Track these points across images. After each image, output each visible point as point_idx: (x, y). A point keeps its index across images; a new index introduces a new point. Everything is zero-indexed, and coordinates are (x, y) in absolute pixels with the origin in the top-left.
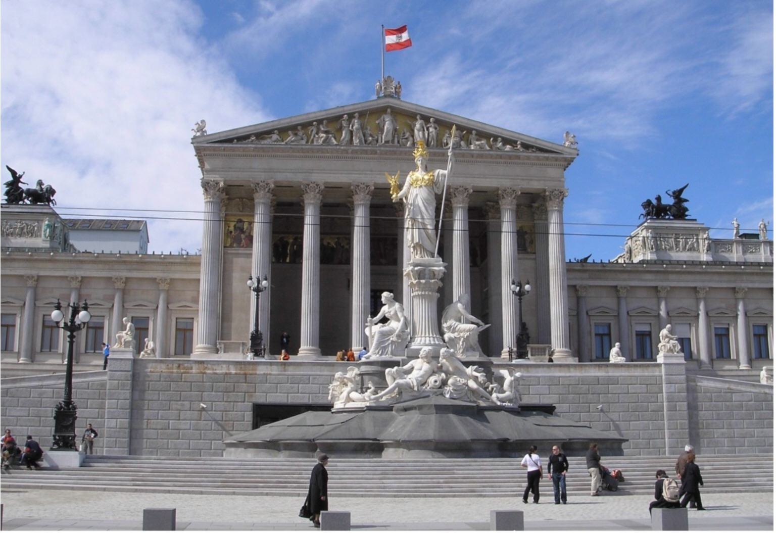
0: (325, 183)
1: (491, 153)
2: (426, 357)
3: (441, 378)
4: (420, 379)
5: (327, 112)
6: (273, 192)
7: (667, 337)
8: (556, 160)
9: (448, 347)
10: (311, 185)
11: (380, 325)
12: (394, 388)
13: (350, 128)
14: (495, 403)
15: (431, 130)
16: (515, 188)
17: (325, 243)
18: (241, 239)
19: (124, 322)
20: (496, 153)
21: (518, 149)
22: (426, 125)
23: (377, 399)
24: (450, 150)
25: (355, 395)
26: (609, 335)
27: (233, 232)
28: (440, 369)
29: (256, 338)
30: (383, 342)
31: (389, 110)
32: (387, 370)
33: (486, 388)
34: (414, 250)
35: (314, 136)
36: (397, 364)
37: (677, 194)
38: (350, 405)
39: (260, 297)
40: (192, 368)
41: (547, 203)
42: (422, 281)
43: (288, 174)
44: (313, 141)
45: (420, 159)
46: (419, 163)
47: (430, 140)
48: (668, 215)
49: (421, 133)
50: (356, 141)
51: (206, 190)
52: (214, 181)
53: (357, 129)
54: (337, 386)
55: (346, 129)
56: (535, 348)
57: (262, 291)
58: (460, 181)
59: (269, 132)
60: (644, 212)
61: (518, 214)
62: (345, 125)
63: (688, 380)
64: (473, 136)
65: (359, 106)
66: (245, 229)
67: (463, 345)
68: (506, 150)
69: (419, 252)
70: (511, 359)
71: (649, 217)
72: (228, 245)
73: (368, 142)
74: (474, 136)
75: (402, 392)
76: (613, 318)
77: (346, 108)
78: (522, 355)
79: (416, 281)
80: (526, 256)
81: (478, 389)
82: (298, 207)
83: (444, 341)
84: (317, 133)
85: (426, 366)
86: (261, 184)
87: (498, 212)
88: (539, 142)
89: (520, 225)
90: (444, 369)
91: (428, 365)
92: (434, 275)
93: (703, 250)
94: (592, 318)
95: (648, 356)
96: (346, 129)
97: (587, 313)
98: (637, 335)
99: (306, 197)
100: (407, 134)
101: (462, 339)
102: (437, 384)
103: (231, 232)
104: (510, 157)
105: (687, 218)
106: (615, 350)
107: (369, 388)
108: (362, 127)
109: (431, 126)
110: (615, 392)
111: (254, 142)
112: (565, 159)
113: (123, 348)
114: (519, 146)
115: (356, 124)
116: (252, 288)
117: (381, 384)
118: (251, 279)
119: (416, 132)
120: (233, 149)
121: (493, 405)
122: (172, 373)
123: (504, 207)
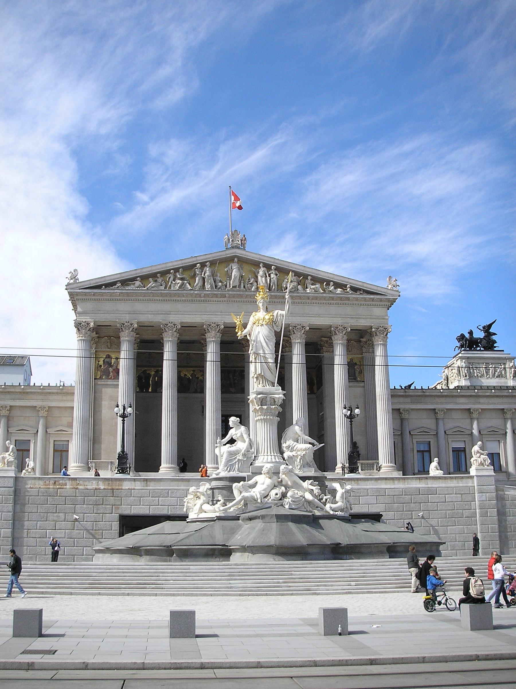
0: (181, 323)
1: (325, 295)
2: (268, 473)
3: (281, 491)
4: (263, 492)
5: (183, 262)
6: (137, 331)
7: (478, 452)
8: (381, 300)
9: (287, 465)
10: (169, 325)
11: (228, 445)
12: (241, 500)
13: (203, 275)
14: (329, 513)
15: (272, 276)
16: (346, 325)
17: (182, 375)
18: (109, 372)
19: (7, 445)
20: (328, 295)
21: (348, 292)
22: (268, 272)
23: (225, 510)
24: (288, 293)
25: (206, 507)
26: (429, 451)
27: (103, 366)
28: (280, 483)
29: (122, 457)
30: (231, 460)
32: (235, 485)
33: (320, 500)
34: (257, 381)
35: (172, 283)
36: (243, 479)
37: (487, 329)
38: (203, 515)
39: (125, 422)
40: (66, 485)
41: (373, 338)
42: (264, 407)
45: (262, 301)
46: (261, 305)
48: (479, 346)
49: (263, 278)
50: (208, 286)
51: (78, 329)
52: (85, 322)
53: (208, 276)
54: (191, 499)
55: (199, 276)
56: (365, 464)
57: (127, 417)
58: (296, 320)
59: (133, 279)
60: (458, 345)
61: (349, 348)
62: (198, 273)
63: (497, 490)
64: (309, 281)
66: (112, 364)
67: (300, 462)
68: (337, 293)
69: (261, 382)
70: (344, 474)
71: (463, 349)
72: (98, 377)
73: (218, 287)
75: (247, 504)
76: (432, 436)
77: (198, 258)
78: (353, 469)
79: (259, 407)
80: (356, 384)
81: (313, 500)
82: (159, 344)
83: (284, 459)
84: (174, 280)
85: (268, 481)
86: (126, 324)
87: (331, 346)
88: (365, 285)
90: (283, 483)
91: (270, 479)
92: (275, 402)
93: (510, 377)
95: (464, 469)
96: (199, 276)
98: (453, 451)
99: (165, 335)
100: (252, 280)
101: (300, 457)
102: (278, 496)
103: (101, 366)
104: (341, 299)
105: (495, 349)
106: (434, 464)
107: (219, 501)
108: (213, 275)
109: (272, 273)
110: (434, 501)
111: (119, 288)
112: (389, 300)
113: (6, 468)
114: (348, 289)
115: (208, 271)
116: (119, 415)
117: (230, 497)
118: (118, 406)
119: (259, 277)
120: (102, 294)
121: (327, 514)
122: (49, 488)
123: (336, 341)
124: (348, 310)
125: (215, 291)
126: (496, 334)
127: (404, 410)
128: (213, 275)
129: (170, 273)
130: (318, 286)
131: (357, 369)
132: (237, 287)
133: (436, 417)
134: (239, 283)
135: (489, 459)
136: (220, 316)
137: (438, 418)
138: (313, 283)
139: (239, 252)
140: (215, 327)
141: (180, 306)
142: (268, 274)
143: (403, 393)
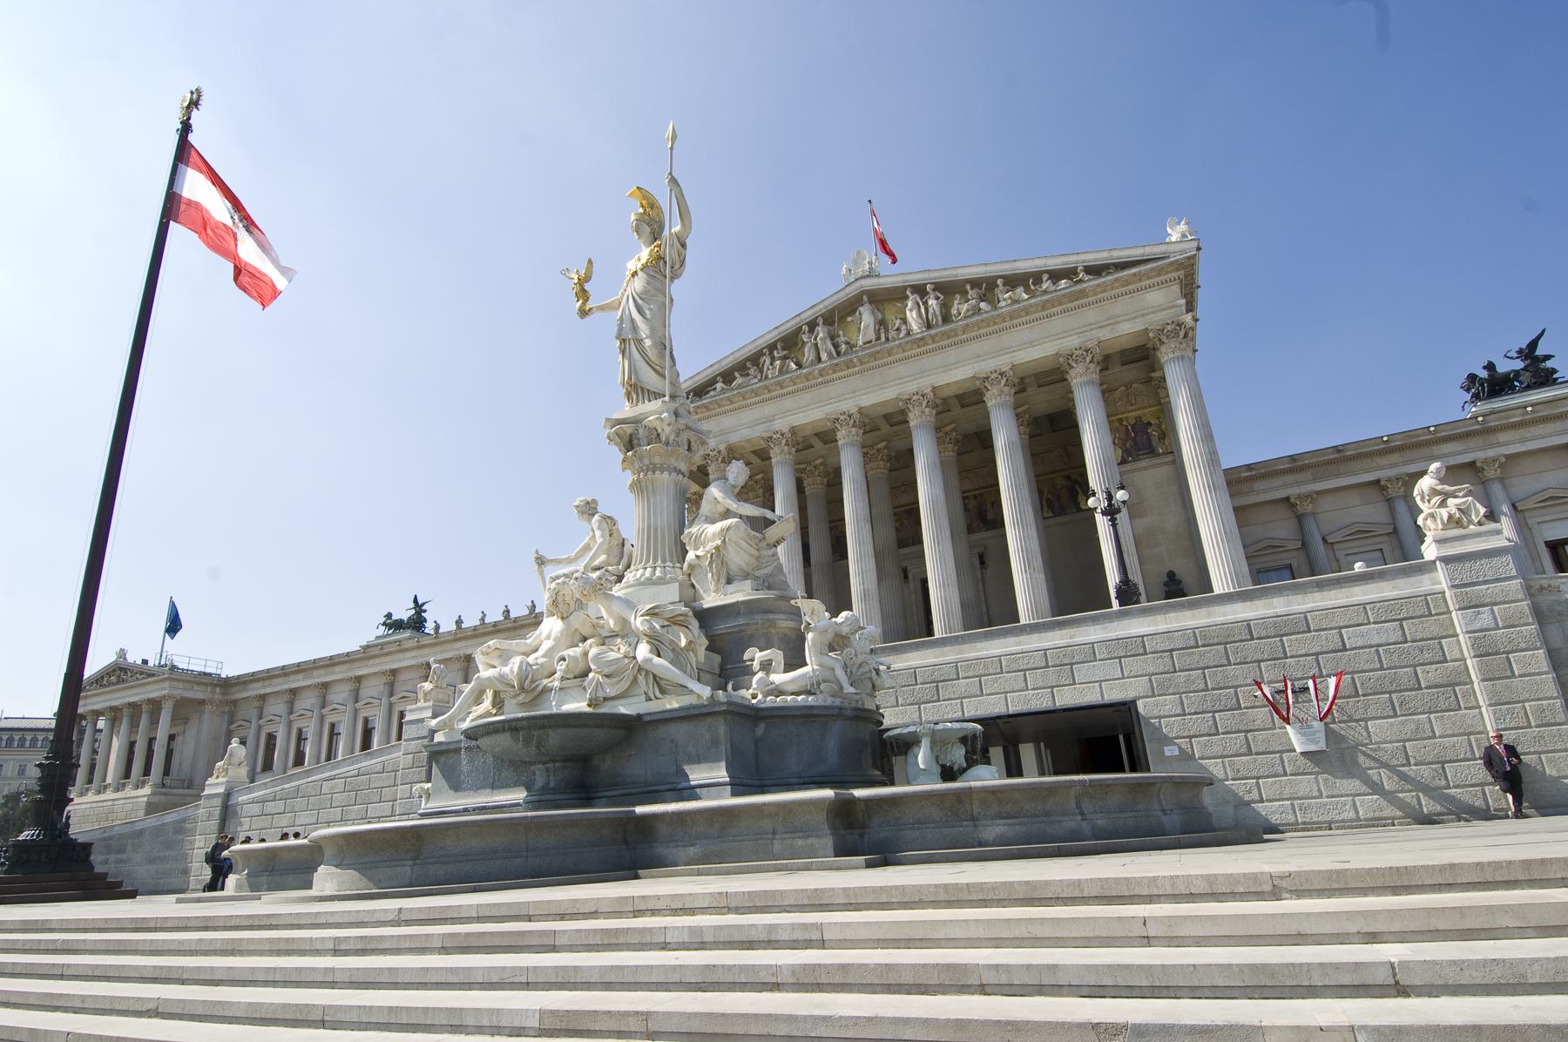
1: (1033, 301)
5: (780, 330)
7: (1434, 492)
15: (932, 302)
16: (1090, 345)
20: (1039, 299)
22: (922, 299)
35: (768, 369)
44: (766, 377)
50: (824, 356)
53: (821, 339)
55: (809, 344)
62: (805, 340)
63: (1529, 589)
65: (821, 306)
74: (1001, 287)
77: (803, 316)
80: (1155, 461)
89: (1135, 414)
94: (1336, 547)
97: (1323, 539)
105: (1560, 380)
108: (833, 338)
110: (1303, 652)
119: (908, 312)
124: (1091, 315)
125: (834, 358)
126: (1553, 356)
127: (1299, 497)
128: (832, 338)
129: (765, 354)
130: (1020, 290)
133: (1385, 497)
134: (876, 334)
135: (1478, 505)
139: (869, 283)
141: (788, 403)
143: (1289, 463)
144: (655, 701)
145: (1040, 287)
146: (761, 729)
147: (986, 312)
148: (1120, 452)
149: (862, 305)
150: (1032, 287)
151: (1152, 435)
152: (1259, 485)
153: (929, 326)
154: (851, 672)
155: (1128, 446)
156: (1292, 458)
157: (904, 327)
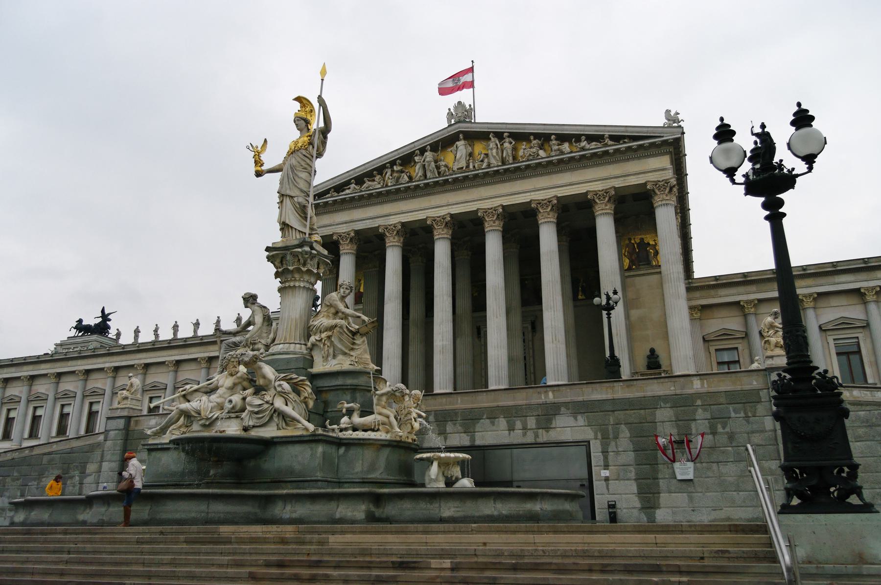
4: (219, 400)
15: (506, 145)
20: (578, 154)
22: (500, 142)
31: (461, 136)
43: (367, 221)
47: (504, 156)
50: (429, 175)
53: (429, 162)
55: (419, 164)
59: (347, 183)
62: (417, 161)
74: (554, 142)
85: (229, 382)
112: (665, 143)
123: (597, 213)
125: (437, 178)
127: (748, 302)
128: (436, 161)
129: (387, 168)
131: (651, 251)
132: (464, 168)
134: (467, 163)
136: (446, 208)
137: (805, 308)
138: (560, 143)
139: (463, 127)
140: (441, 221)
142: (501, 145)
143: (741, 278)
144: (282, 431)
145: (579, 145)
146: (342, 450)
147: (542, 158)
148: (627, 262)
149: (459, 141)
150: (574, 144)
151: (649, 252)
152: (723, 292)
153: (504, 163)
154: (400, 419)
155: (633, 258)
156: (744, 275)
157: (486, 160)
